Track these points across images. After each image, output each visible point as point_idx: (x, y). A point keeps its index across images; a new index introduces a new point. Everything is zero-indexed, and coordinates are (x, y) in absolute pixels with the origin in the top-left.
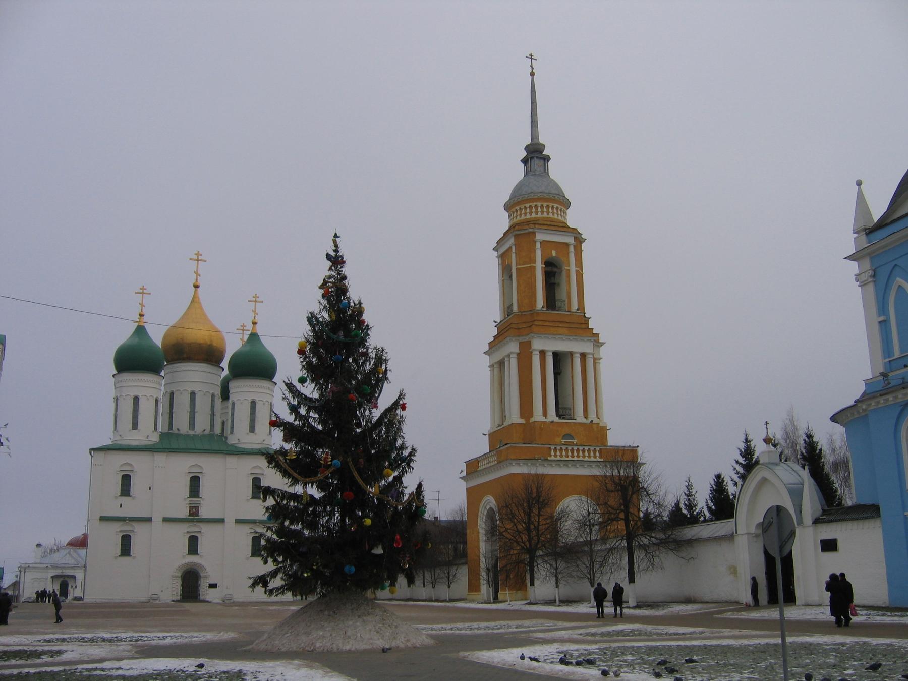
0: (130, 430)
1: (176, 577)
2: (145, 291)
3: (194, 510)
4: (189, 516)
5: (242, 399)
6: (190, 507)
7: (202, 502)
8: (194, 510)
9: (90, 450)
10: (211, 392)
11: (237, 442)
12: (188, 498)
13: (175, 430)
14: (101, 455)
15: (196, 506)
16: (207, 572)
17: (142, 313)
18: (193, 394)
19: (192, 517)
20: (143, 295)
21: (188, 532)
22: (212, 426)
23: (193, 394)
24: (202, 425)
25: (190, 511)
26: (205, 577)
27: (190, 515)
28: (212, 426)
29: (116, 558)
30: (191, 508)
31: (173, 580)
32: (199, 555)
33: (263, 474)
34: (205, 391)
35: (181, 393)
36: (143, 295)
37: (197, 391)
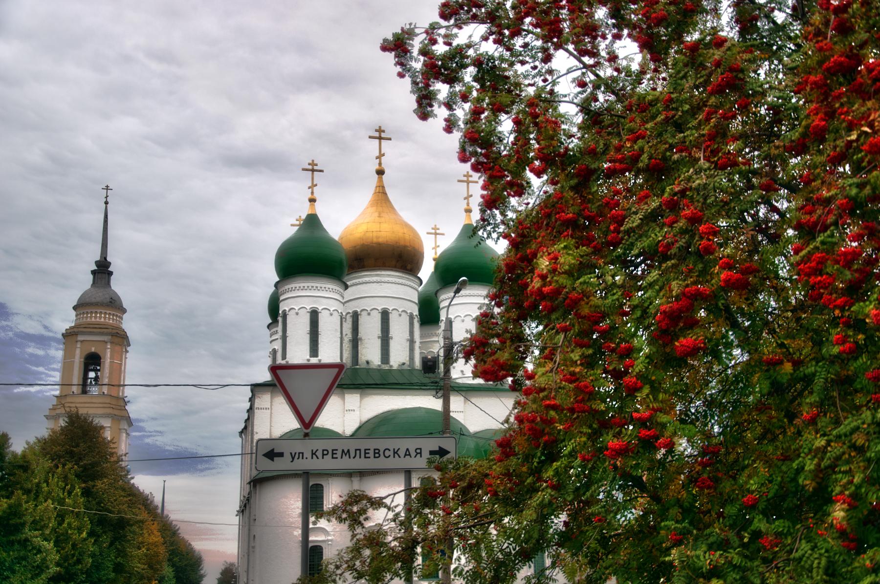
2: (315, 168)
5: (462, 316)
10: (409, 312)
11: (460, 375)
13: (364, 366)
17: (313, 197)
18: (385, 315)
20: (313, 174)
22: (412, 358)
23: (385, 315)
24: (399, 356)
28: (412, 358)
34: (400, 310)
35: (369, 314)
36: (313, 174)
37: (391, 309)
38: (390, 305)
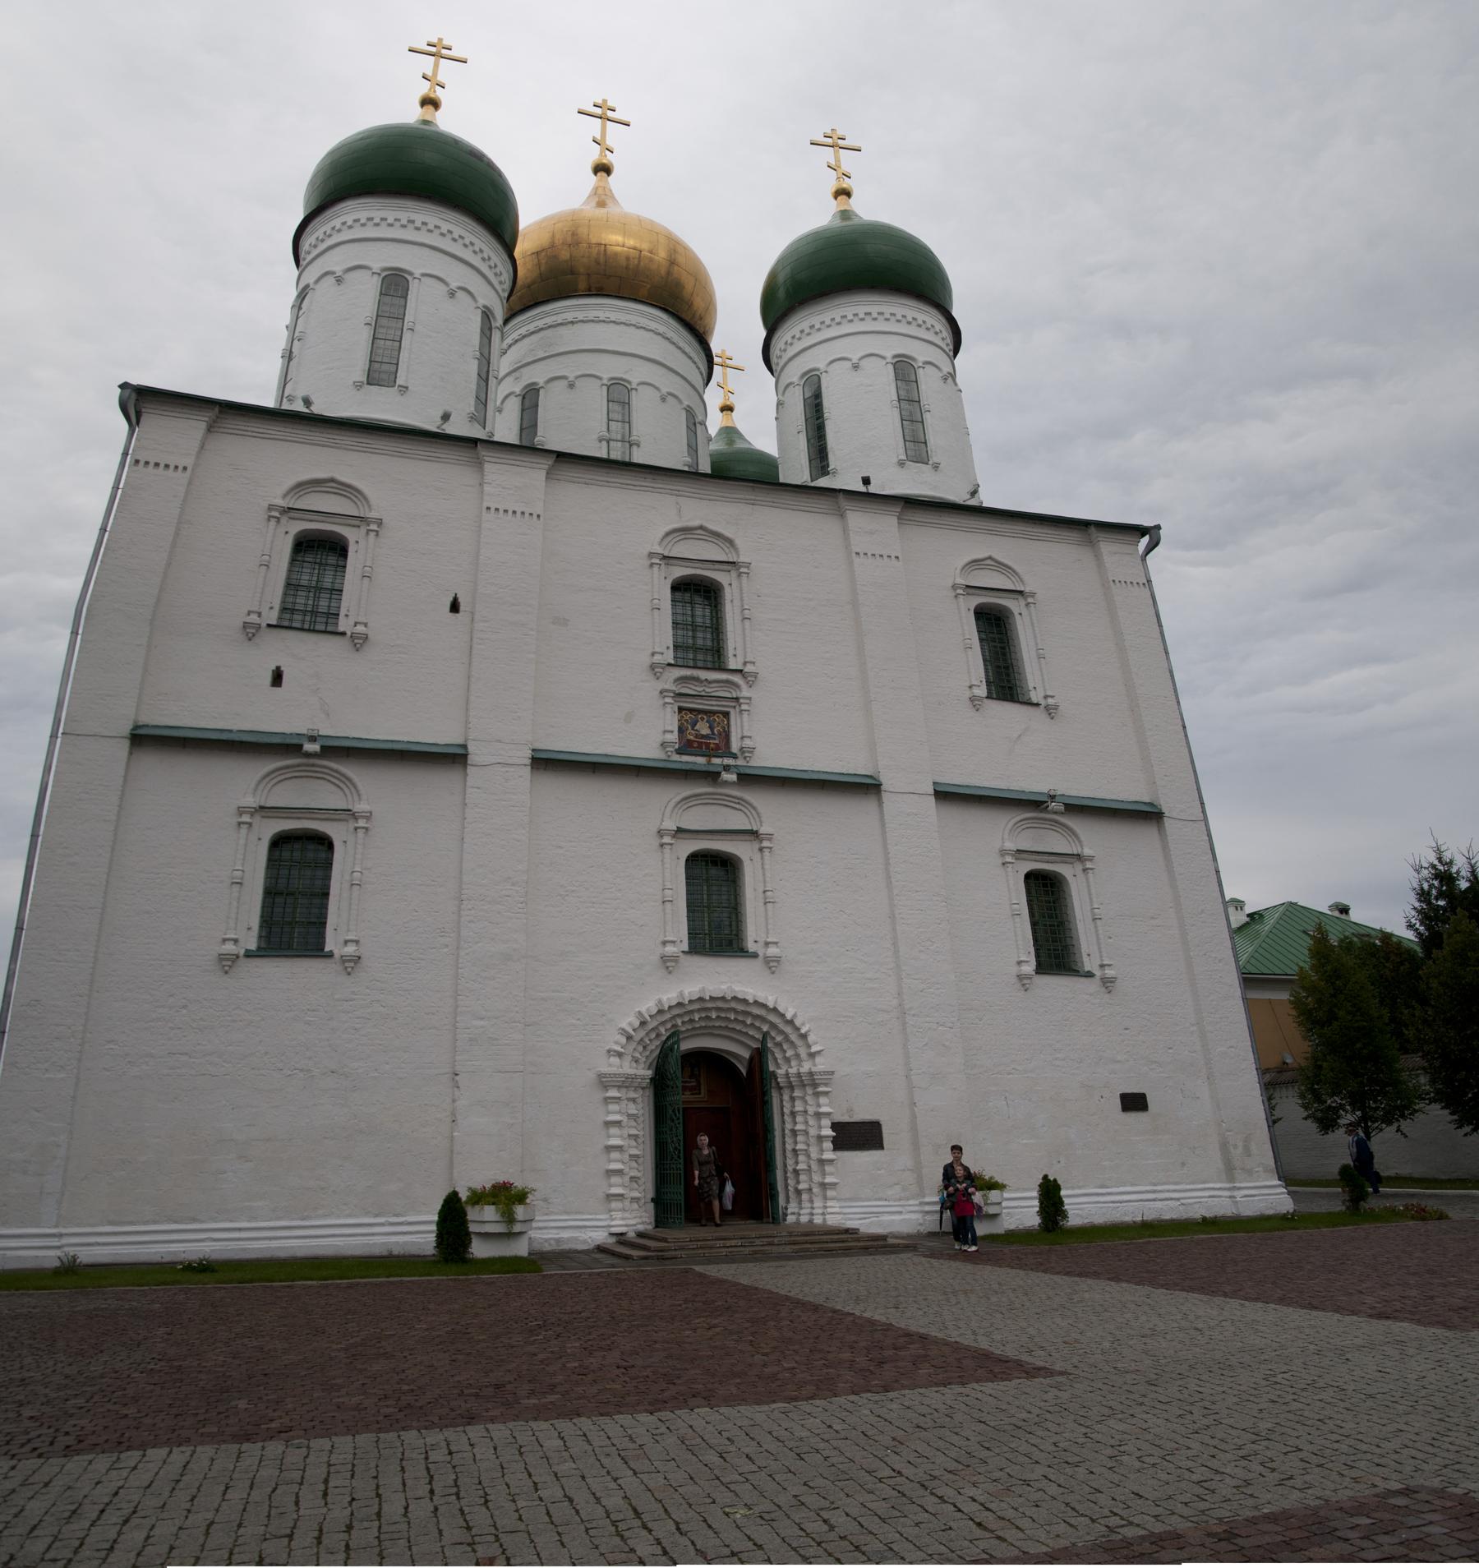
0: (358, 386)
1: (626, 1083)
3: (705, 731)
4: (679, 752)
6: (681, 709)
7: (745, 692)
8: (703, 728)
9: (120, 386)
12: (669, 665)
14: (190, 429)
15: (713, 705)
16: (812, 1056)
19: (701, 760)
21: (680, 830)
25: (681, 730)
26: (811, 1082)
27: (686, 746)
29: (227, 963)
30: (688, 714)
31: (607, 1100)
32: (755, 956)
33: (1021, 592)
38: (637, 373)
